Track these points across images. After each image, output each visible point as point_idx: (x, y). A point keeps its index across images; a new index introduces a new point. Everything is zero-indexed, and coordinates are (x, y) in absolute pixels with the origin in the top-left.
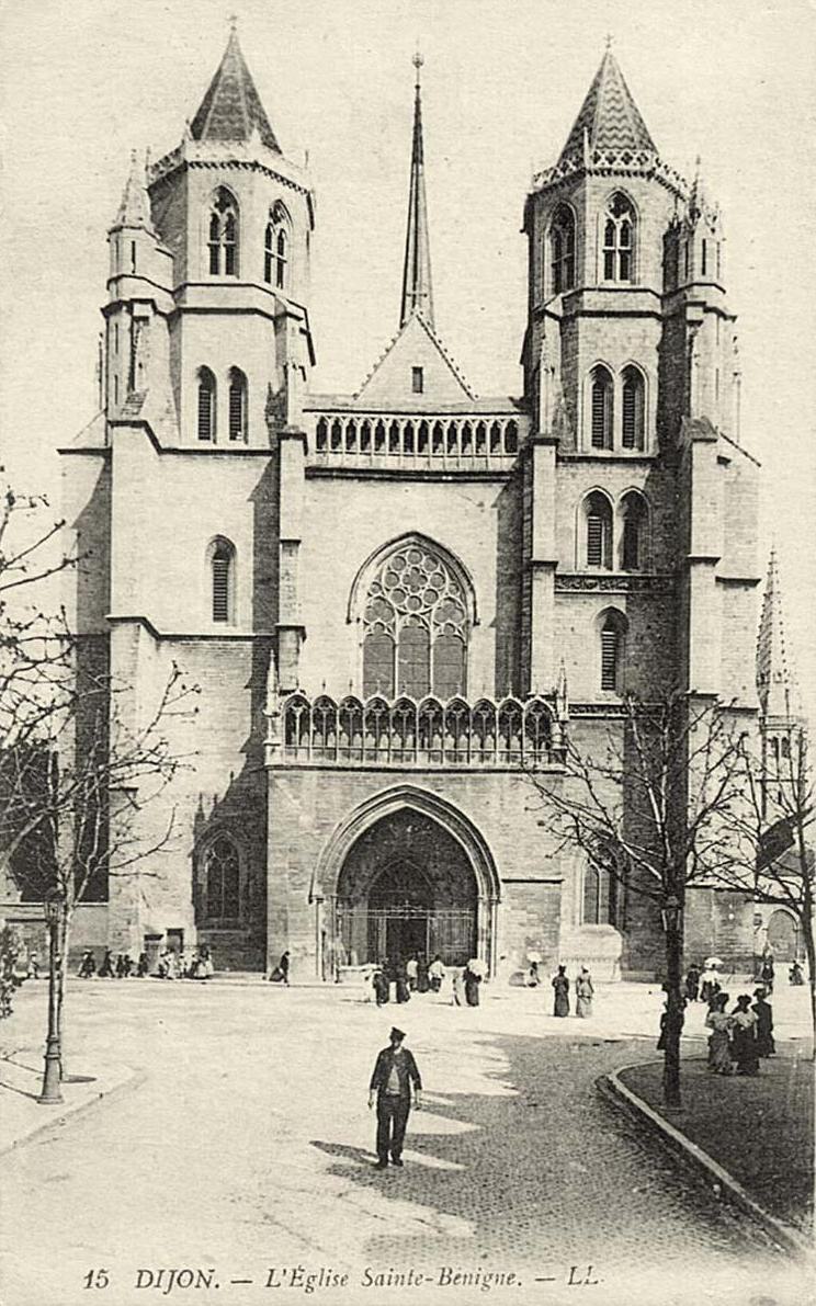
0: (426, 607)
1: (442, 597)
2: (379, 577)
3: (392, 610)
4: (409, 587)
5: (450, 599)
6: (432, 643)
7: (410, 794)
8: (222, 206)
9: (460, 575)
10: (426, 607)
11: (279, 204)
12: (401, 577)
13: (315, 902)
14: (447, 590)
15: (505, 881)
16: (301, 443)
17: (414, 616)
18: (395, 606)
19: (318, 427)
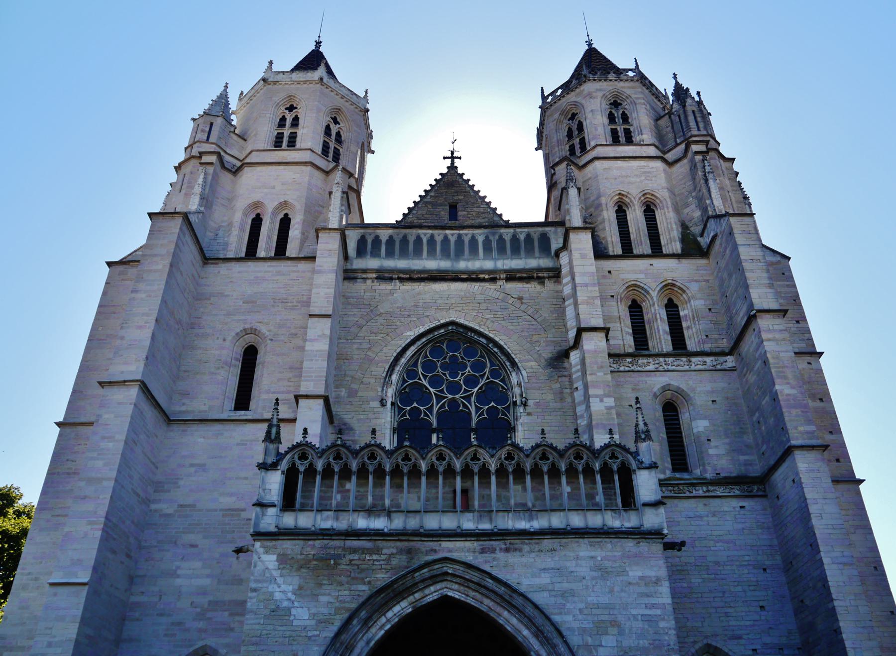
12: (438, 364)
18: (432, 390)
19: (359, 241)
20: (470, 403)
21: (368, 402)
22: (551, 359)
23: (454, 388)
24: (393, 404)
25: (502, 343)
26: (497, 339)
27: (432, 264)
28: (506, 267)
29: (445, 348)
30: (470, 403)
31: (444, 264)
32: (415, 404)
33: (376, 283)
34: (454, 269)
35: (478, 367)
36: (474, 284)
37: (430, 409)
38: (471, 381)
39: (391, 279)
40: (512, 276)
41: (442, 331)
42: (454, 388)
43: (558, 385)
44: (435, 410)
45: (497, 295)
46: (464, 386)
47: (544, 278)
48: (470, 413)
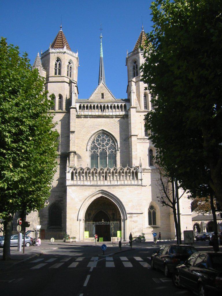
0: (106, 147)
1: (109, 145)
2: (94, 140)
3: (97, 147)
4: (101, 142)
5: (111, 145)
6: (107, 155)
7: (103, 192)
8: (58, 61)
9: (114, 140)
10: (106, 147)
11: (71, 60)
13: (79, 221)
14: (111, 142)
15: (128, 214)
16: (75, 109)
17: (103, 149)
18: (98, 146)
20: (107, 150)
21: (84, 150)
22: (125, 139)
23: (103, 146)
24: (89, 150)
25: (114, 135)
26: (112, 134)
27: (97, 114)
28: (115, 114)
29: (101, 135)
30: (107, 150)
31: (100, 113)
32: (94, 150)
33: (84, 118)
34: (103, 115)
35: (109, 140)
36: (108, 119)
37: (98, 151)
38: (107, 144)
39: (88, 117)
40: (117, 116)
41: (100, 131)
42: (103, 146)
43: (126, 146)
44: (99, 151)
45: (113, 122)
46: (105, 146)
47: (124, 117)
48: (106, 153)
